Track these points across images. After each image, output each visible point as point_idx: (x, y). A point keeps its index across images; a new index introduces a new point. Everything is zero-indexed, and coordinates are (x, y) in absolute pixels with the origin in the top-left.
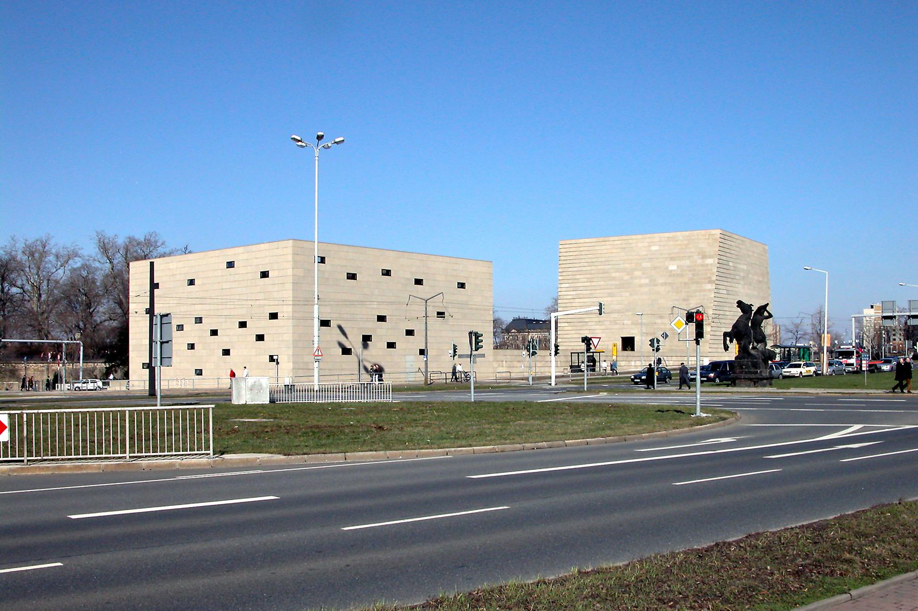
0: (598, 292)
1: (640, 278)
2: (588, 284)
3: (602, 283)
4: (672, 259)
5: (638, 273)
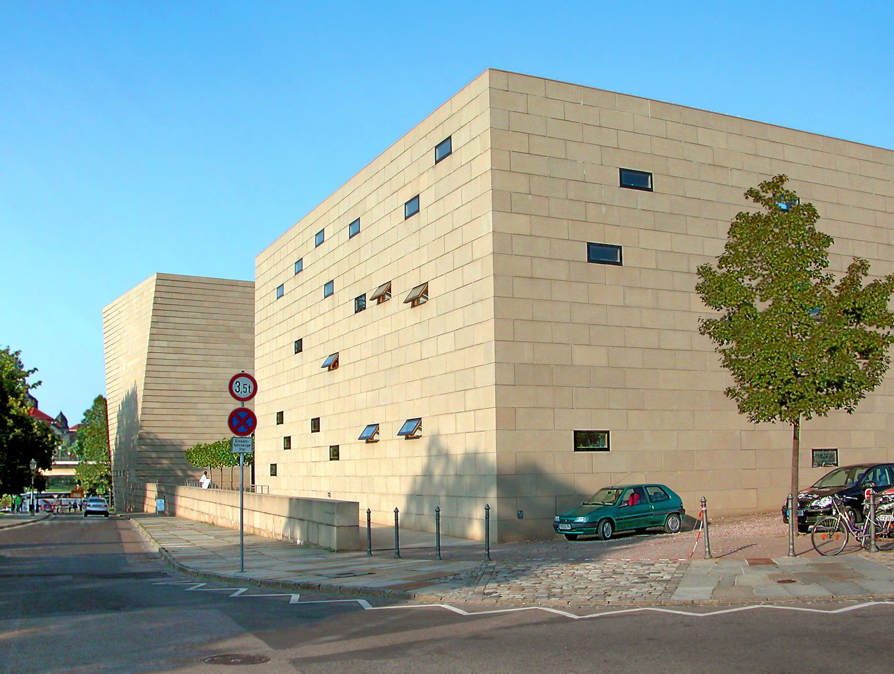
2: (201, 345)
3: (225, 346)
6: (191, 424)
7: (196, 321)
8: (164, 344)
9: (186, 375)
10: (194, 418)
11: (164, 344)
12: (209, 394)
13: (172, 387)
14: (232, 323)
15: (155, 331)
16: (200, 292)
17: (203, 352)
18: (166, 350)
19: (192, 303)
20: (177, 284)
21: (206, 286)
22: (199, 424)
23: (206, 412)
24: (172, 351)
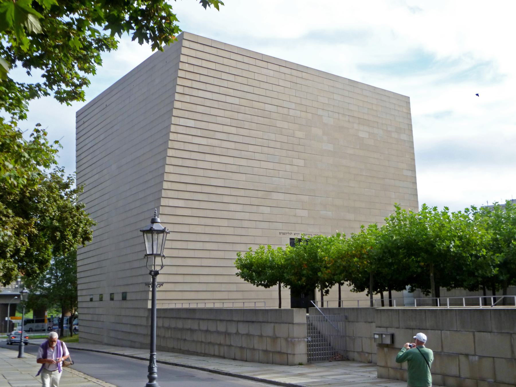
2: (233, 130)
6: (223, 231)
7: (229, 99)
8: (191, 123)
9: (215, 166)
10: (225, 223)
11: (191, 123)
12: (241, 193)
13: (199, 181)
14: (268, 107)
16: (233, 63)
19: (224, 76)
20: (207, 49)
21: (239, 58)
22: (230, 231)
23: (238, 216)
24: (199, 133)
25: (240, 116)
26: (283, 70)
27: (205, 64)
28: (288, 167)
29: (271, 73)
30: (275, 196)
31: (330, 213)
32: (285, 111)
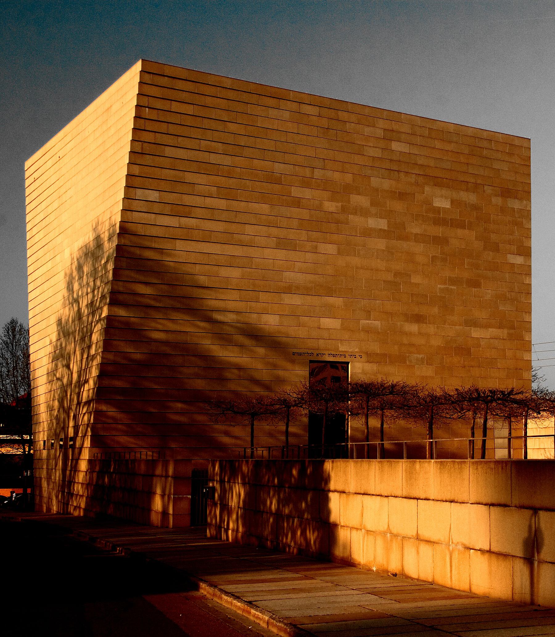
0: (249, 229)
1: (364, 213)
2: (222, 204)
3: (265, 208)
4: (438, 182)
5: (360, 200)
7: (213, 158)
8: (154, 196)
11: (154, 196)
14: (279, 168)
15: (136, 170)
16: (223, 103)
17: (224, 216)
18: (156, 208)
19: (206, 124)
20: (180, 85)
25: (232, 182)
26: (307, 109)
27: (175, 107)
28: (310, 256)
29: (287, 115)
30: (288, 299)
31: (377, 323)
32: (308, 172)
